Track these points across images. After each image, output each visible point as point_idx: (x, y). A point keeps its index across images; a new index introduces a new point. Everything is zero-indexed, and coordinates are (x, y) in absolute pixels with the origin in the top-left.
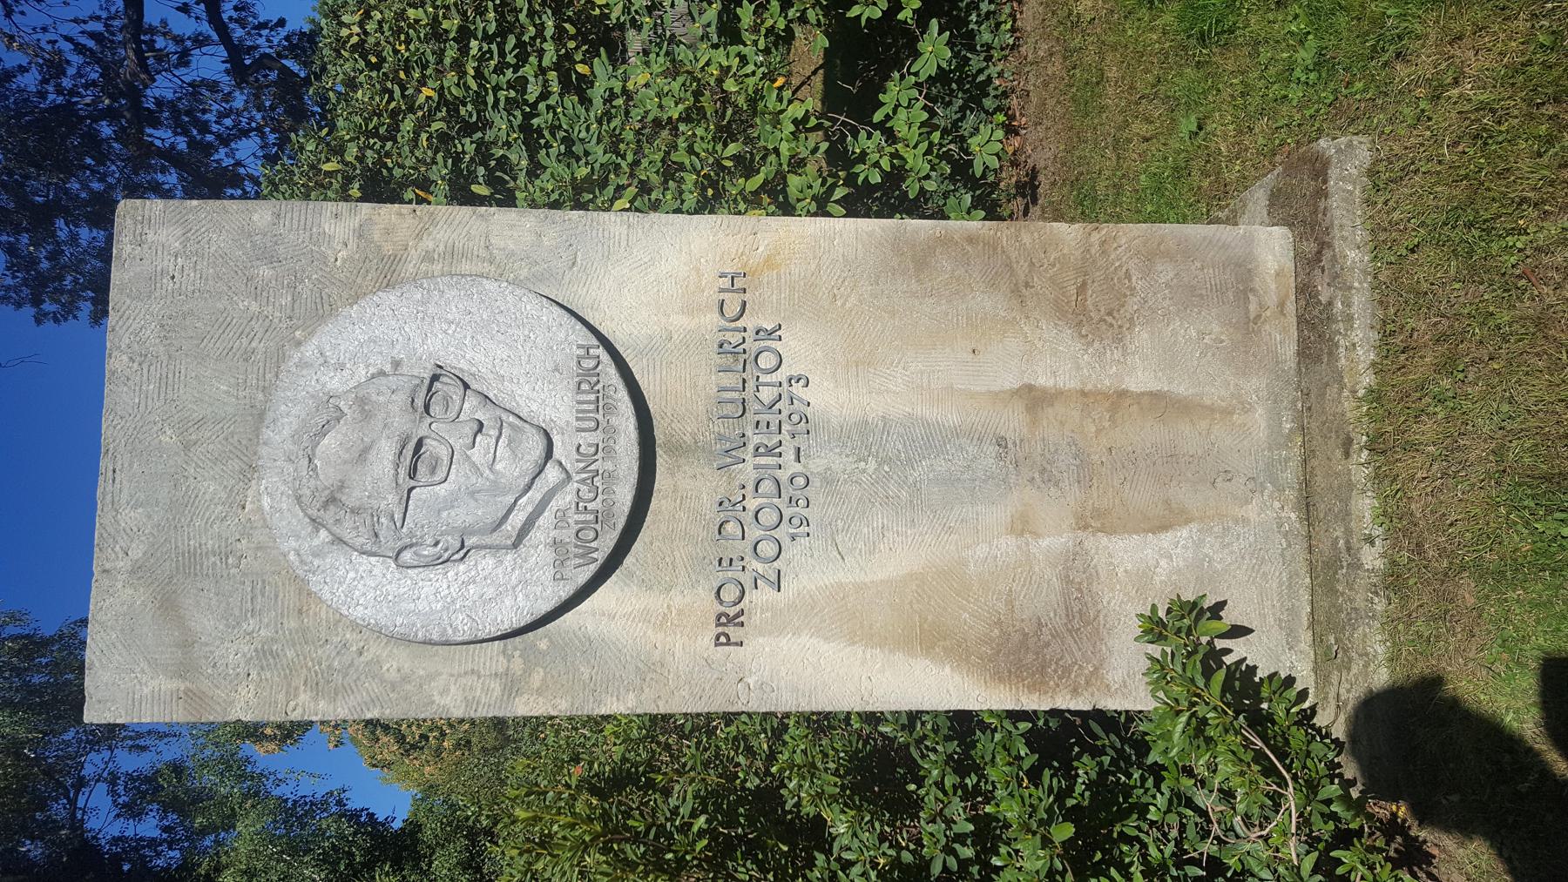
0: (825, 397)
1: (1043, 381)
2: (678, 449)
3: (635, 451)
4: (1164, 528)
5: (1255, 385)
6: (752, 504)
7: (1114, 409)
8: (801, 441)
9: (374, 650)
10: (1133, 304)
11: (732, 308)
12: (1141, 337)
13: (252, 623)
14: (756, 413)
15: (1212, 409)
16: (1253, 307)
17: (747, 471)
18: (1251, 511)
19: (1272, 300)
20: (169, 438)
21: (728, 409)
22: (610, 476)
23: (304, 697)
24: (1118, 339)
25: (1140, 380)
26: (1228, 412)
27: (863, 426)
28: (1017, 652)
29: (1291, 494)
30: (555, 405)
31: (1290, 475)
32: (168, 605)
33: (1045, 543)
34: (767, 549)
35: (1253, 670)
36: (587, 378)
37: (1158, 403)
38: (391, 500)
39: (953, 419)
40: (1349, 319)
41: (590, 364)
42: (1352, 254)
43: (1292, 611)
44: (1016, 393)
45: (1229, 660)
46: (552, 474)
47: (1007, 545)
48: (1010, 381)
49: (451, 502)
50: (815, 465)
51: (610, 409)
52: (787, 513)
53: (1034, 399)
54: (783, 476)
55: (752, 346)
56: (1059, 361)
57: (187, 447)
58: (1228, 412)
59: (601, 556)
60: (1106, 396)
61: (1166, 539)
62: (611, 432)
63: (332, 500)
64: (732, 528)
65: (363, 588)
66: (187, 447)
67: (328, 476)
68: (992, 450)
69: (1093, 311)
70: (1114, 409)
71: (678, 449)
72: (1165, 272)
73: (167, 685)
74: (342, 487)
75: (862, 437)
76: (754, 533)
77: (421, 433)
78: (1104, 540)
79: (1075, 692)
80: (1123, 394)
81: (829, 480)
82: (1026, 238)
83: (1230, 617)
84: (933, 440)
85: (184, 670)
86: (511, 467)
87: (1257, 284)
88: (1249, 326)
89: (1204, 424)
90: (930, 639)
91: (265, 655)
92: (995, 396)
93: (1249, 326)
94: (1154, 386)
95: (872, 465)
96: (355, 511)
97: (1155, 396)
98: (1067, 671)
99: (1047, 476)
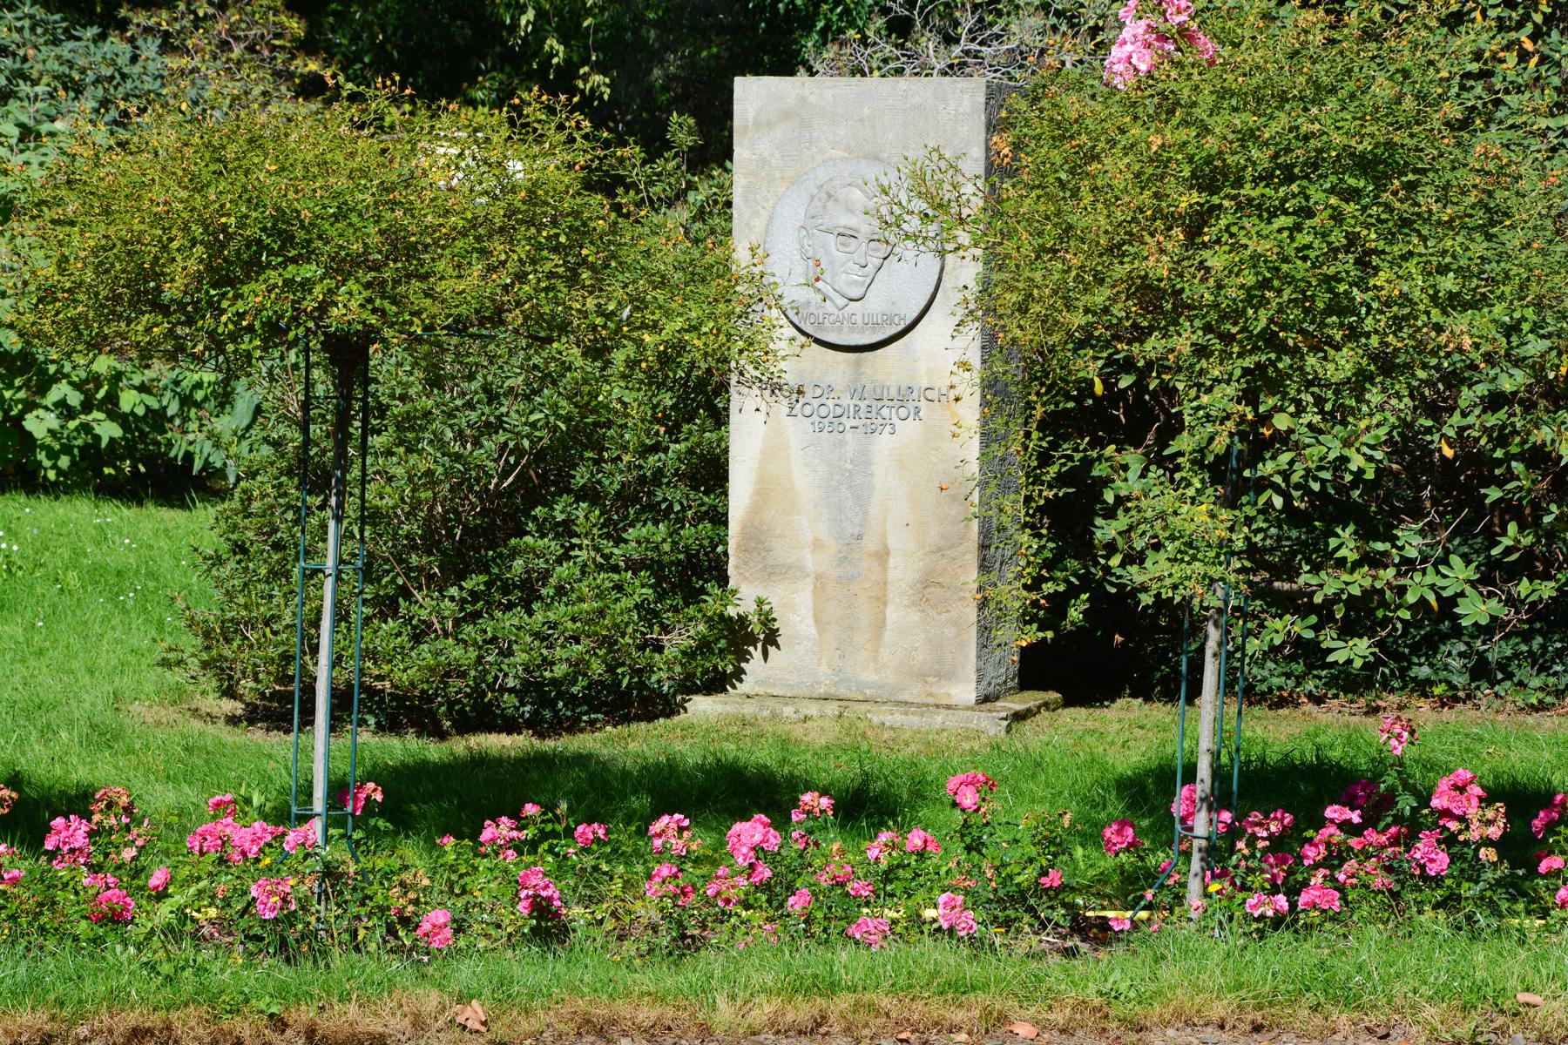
0: (883, 443)
1: (892, 561)
2: (858, 364)
3: (852, 343)
4: (816, 620)
5: (890, 677)
6: (830, 403)
7: (878, 599)
8: (861, 430)
9: (765, 215)
10: (932, 612)
11: (930, 394)
12: (915, 617)
13: (778, 155)
14: (880, 406)
15: (876, 651)
16: (930, 679)
17: (846, 401)
18: (824, 668)
19: (934, 690)
20: (867, 111)
21: (878, 392)
22: (840, 330)
23: (744, 182)
24: (914, 603)
25: (893, 614)
26: (875, 660)
27: (868, 463)
28: (756, 539)
29: (832, 691)
30: (876, 303)
31: (842, 691)
32: (787, 115)
33: (809, 557)
34: (808, 410)
35: (747, 661)
36: (889, 319)
37: (880, 625)
38: (827, 222)
39: (874, 510)
40: (906, 713)
41: (896, 320)
42: (939, 719)
43: (774, 685)
44: (885, 546)
45: (751, 649)
46: (841, 301)
47: (808, 537)
48: (892, 544)
49: (827, 252)
50: (849, 436)
51: (874, 330)
52: (826, 421)
53: (883, 556)
54: (843, 419)
55: (911, 405)
56: (903, 570)
57: (862, 120)
58: (875, 660)
59: (802, 326)
60: (884, 595)
61: (810, 621)
62: (862, 331)
63: (830, 196)
64: (818, 392)
65: (792, 213)
66: (862, 120)
67: (841, 193)
68: (856, 531)
69: (928, 588)
70: (878, 599)
71: (858, 364)
72: (950, 632)
73: (751, 116)
74: (836, 200)
75: (864, 462)
76: (816, 403)
77: (861, 239)
78: (811, 588)
79: (737, 567)
80: (885, 604)
81: (841, 443)
82: (968, 556)
83: (772, 650)
84: (862, 498)
85: (758, 125)
86: (842, 281)
87: (944, 682)
88: (921, 676)
89: (869, 646)
90: (763, 493)
91: (763, 162)
92: (884, 535)
93: (921, 676)
94: (889, 621)
95: (849, 467)
96: (824, 207)
97: (884, 621)
98: (746, 563)
99: (843, 560)
